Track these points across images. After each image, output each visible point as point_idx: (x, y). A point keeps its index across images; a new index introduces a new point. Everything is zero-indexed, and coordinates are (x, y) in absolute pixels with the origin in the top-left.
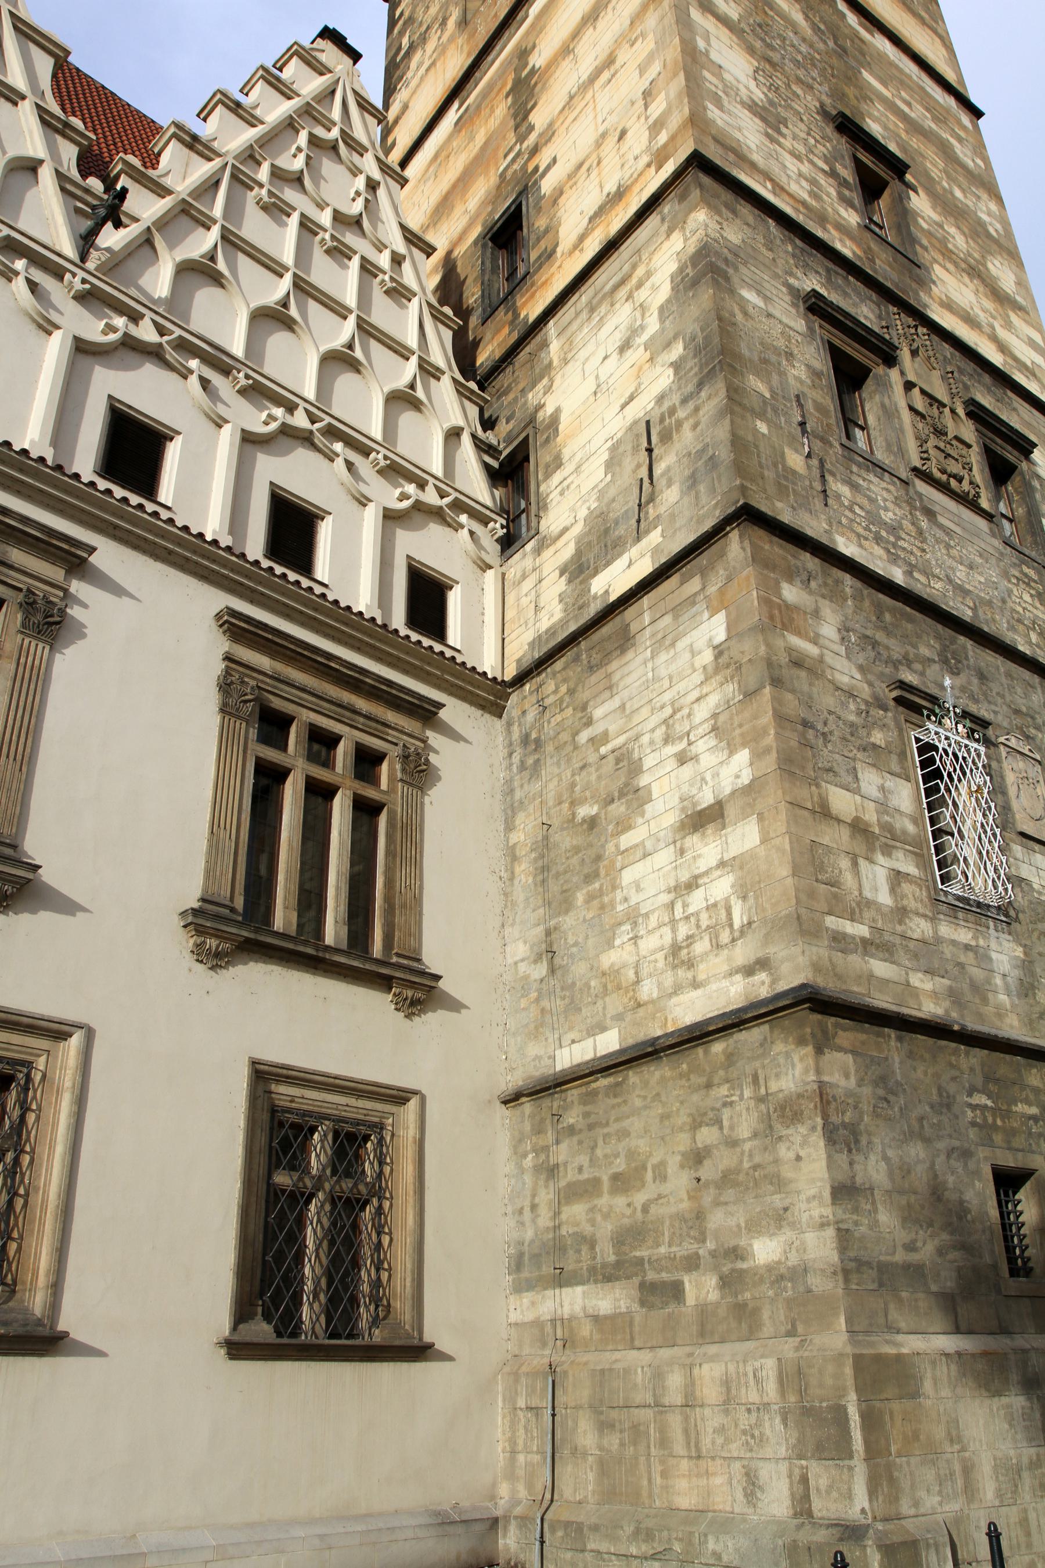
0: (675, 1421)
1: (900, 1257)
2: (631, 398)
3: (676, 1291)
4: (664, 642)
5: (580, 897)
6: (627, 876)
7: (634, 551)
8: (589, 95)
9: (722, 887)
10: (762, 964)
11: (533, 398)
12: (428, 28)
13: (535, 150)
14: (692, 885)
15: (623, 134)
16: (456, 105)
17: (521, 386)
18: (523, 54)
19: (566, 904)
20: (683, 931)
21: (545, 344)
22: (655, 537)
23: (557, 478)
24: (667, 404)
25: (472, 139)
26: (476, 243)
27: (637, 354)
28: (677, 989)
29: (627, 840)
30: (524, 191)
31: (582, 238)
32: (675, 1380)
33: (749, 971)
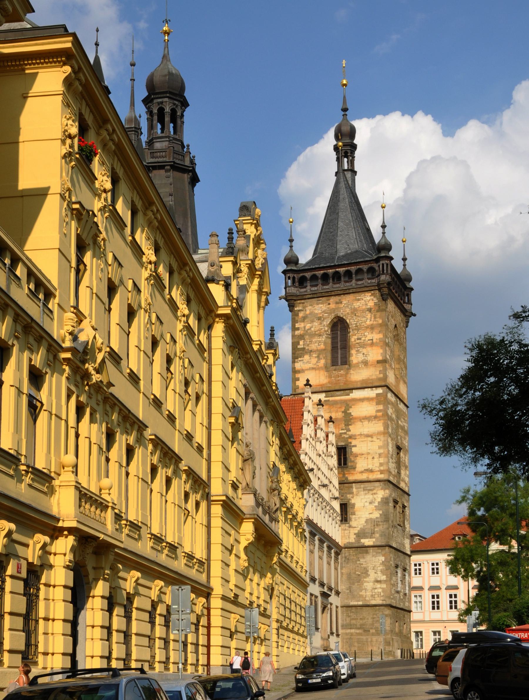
2: (371, 513)
3: (369, 631)
4: (373, 556)
5: (356, 584)
6: (365, 584)
7: (370, 540)
8: (366, 439)
9: (380, 590)
10: (384, 600)
11: (349, 496)
12: (311, 351)
14: (376, 589)
15: (373, 458)
17: (346, 491)
18: (348, 405)
19: (353, 584)
20: (373, 594)
21: (352, 487)
22: (374, 540)
23: (354, 516)
24: (378, 520)
27: (373, 506)
28: (372, 600)
29: (365, 579)
31: (362, 472)
33: (383, 600)
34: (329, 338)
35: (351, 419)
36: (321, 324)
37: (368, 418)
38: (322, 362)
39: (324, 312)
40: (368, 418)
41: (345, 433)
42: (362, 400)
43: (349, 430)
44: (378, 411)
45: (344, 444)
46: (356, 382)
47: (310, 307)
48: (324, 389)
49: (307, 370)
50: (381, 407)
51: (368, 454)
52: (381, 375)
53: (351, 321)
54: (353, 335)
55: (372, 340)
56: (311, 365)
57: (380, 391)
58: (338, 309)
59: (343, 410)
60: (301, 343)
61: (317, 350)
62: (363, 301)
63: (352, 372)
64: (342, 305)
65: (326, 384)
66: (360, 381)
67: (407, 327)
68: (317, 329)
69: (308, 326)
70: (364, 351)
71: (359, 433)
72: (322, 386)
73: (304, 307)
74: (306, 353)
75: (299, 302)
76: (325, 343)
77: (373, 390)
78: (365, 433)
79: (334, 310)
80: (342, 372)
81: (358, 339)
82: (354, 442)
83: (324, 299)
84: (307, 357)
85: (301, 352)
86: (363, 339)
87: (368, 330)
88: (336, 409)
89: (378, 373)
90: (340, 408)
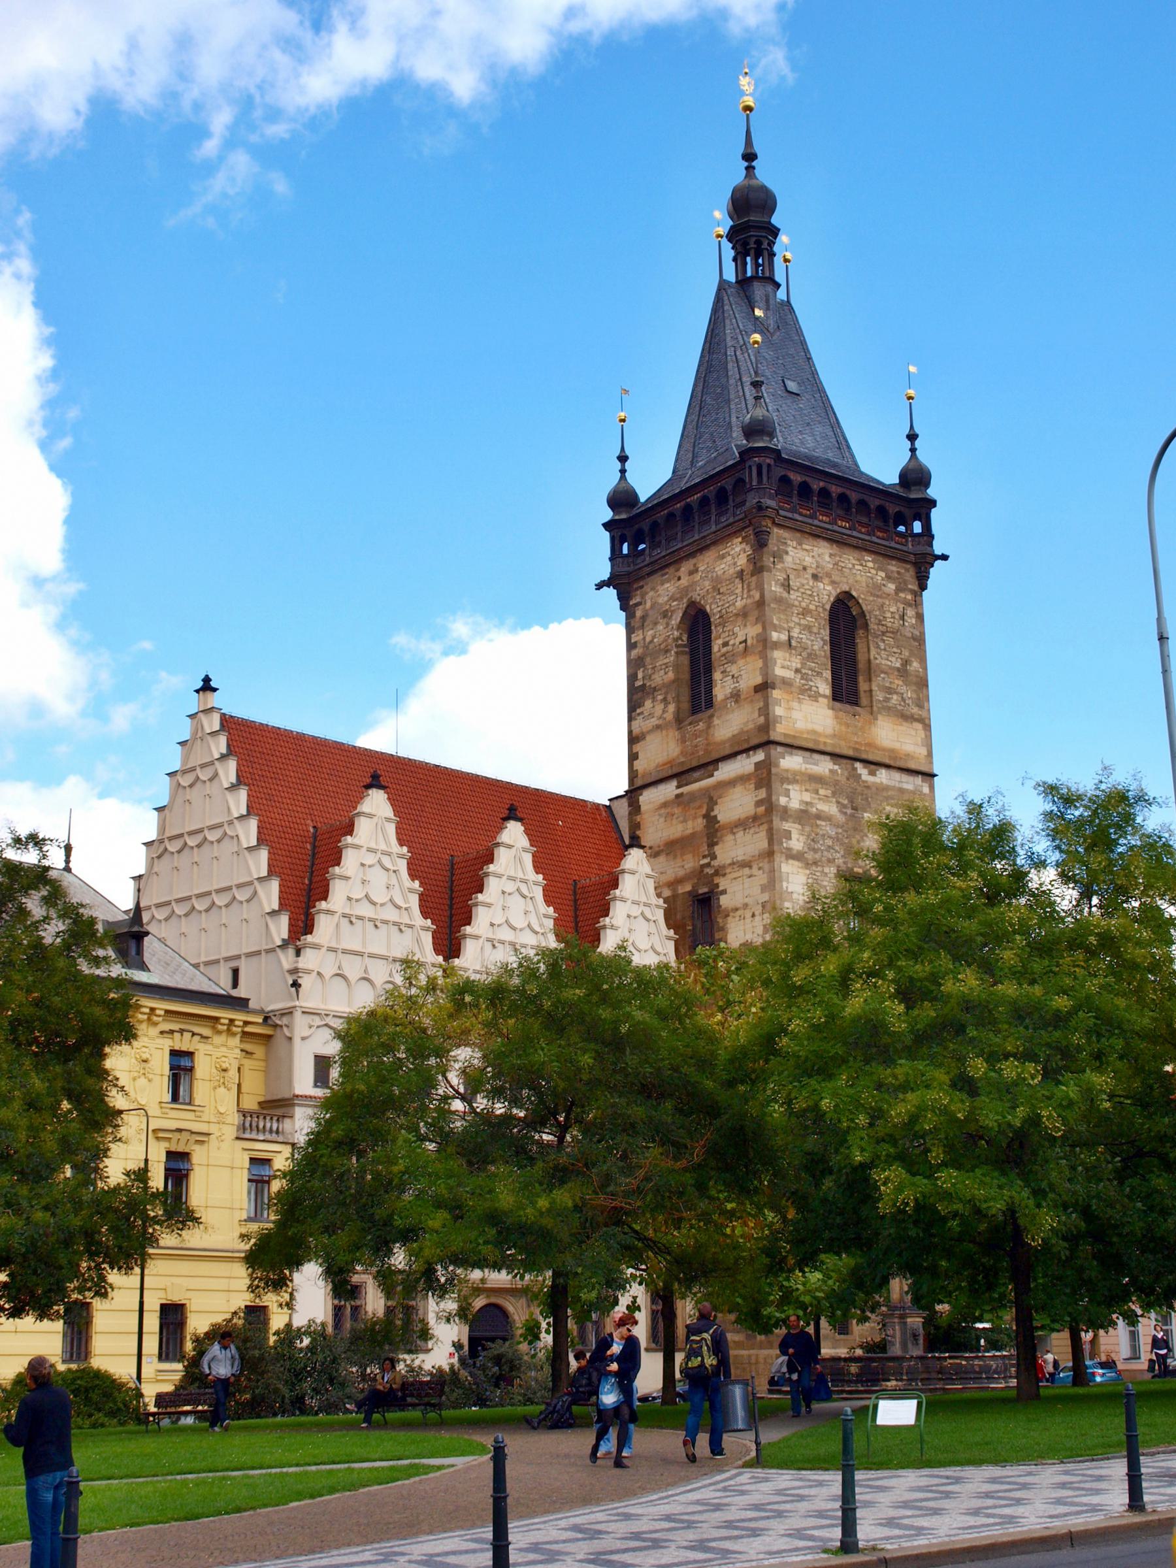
0: (753, 1367)
8: (740, 873)
12: (655, 689)
13: (717, 873)
15: (753, 915)
16: (674, 783)
18: (710, 799)
25: (685, 821)
26: (689, 892)
30: (711, 892)
32: (753, 1358)
34: (686, 653)
35: (717, 831)
36: (668, 624)
37: (743, 824)
38: (672, 708)
39: (672, 598)
40: (743, 824)
41: (708, 865)
42: (731, 783)
43: (714, 857)
44: (759, 803)
45: (706, 890)
46: (723, 742)
47: (651, 594)
48: (676, 770)
49: (649, 732)
50: (762, 794)
51: (746, 906)
52: (762, 719)
53: (712, 608)
54: (716, 639)
55: (745, 641)
56: (654, 721)
57: (760, 756)
58: (692, 585)
59: (704, 811)
60: (640, 675)
61: (664, 685)
62: (729, 558)
63: (716, 721)
64: (697, 577)
65: (678, 757)
66: (729, 739)
67: (923, 587)
68: (662, 638)
69: (651, 632)
70: (733, 669)
71: (729, 861)
72: (670, 763)
73: (643, 597)
74: (648, 694)
75: (635, 586)
76: (676, 667)
77: (748, 757)
78: (740, 858)
79: (685, 591)
80: (701, 726)
81: (725, 644)
82: (723, 883)
83: (671, 570)
84: (648, 704)
85: (640, 694)
86: (731, 643)
87: (740, 621)
88: (693, 812)
89: (756, 714)
90: (700, 807)
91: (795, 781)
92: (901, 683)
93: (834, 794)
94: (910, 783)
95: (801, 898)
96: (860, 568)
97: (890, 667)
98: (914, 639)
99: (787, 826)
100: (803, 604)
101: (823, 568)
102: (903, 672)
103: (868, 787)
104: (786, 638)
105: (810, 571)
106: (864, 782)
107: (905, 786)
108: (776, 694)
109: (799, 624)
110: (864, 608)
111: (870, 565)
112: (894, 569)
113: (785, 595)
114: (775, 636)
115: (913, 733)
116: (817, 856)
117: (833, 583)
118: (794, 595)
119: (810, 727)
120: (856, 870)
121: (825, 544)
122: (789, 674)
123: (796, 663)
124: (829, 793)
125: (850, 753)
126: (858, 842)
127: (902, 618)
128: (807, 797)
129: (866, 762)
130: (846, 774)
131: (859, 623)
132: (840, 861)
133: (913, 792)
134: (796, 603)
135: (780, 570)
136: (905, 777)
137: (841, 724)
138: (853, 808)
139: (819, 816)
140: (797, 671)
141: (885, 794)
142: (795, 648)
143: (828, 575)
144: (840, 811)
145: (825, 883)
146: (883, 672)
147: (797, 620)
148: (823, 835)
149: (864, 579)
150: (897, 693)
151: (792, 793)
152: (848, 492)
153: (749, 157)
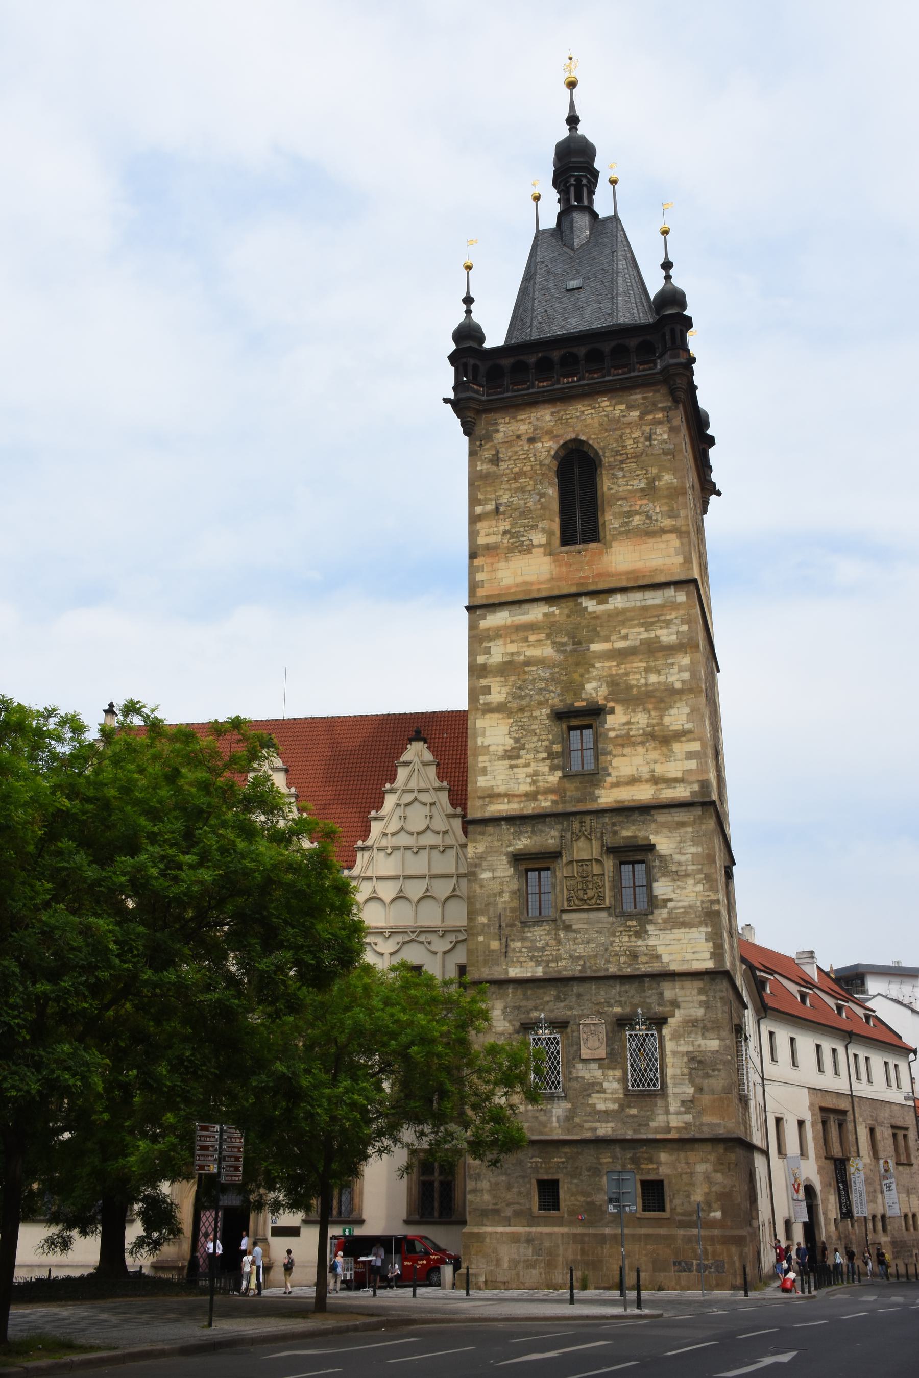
1: (490, 1207)
91: (501, 636)
92: (645, 502)
93: (548, 636)
94: (654, 598)
95: (501, 749)
96: (593, 411)
97: (630, 492)
98: (665, 453)
99: (483, 682)
100: (517, 469)
101: (541, 428)
102: (650, 491)
103: (597, 617)
104: (494, 507)
105: (524, 438)
106: (590, 613)
107: (650, 602)
108: (477, 562)
109: (510, 490)
110: (596, 446)
111: (607, 403)
112: (639, 396)
113: (494, 468)
114: (479, 510)
115: (663, 546)
116: (524, 703)
117: (554, 437)
118: (503, 466)
119: (519, 580)
120: (576, 704)
121: (547, 406)
122: (492, 539)
123: (505, 525)
124: (542, 636)
125: (574, 590)
126: (582, 676)
127: (649, 438)
128: (512, 648)
129: (592, 594)
130: (566, 611)
131: (597, 463)
132: (556, 700)
133: (662, 607)
134: (508, 471)
135: (488, 449)
136: (649, 594)
137: (560, 566)
138: (574, 644)
139: (528, 663)
140: (505, 533)
141: (620, 618)
142: (504, 513)
143: (549, 432)
144: (558, 651)
145: (534, 727)
146: (619, 499)
147: (507, 487)
148: (535, 679)
149: (596, 420)
150: (637, 513)
151: (493, 651)
152: (575, 350)
153: (573, 121)
